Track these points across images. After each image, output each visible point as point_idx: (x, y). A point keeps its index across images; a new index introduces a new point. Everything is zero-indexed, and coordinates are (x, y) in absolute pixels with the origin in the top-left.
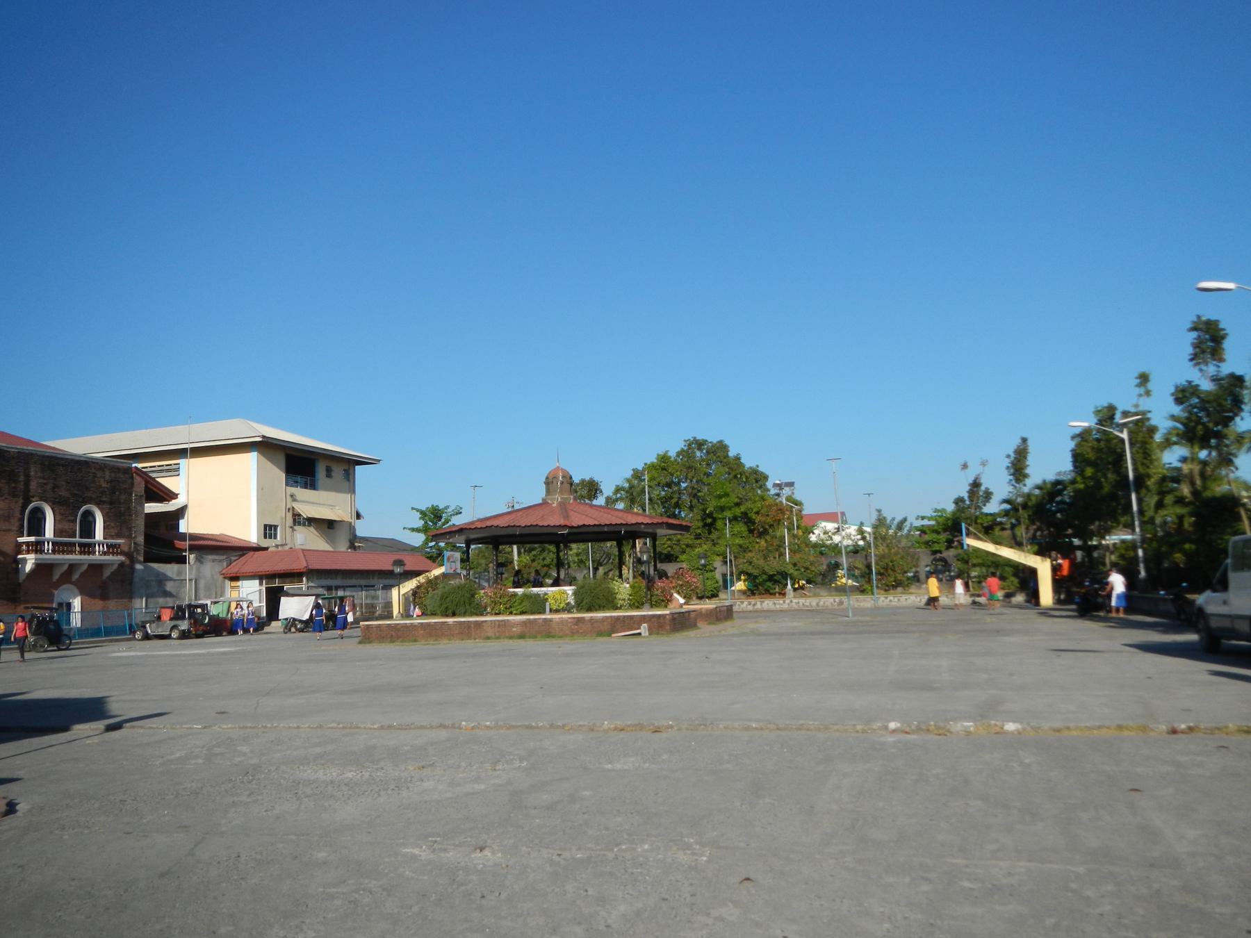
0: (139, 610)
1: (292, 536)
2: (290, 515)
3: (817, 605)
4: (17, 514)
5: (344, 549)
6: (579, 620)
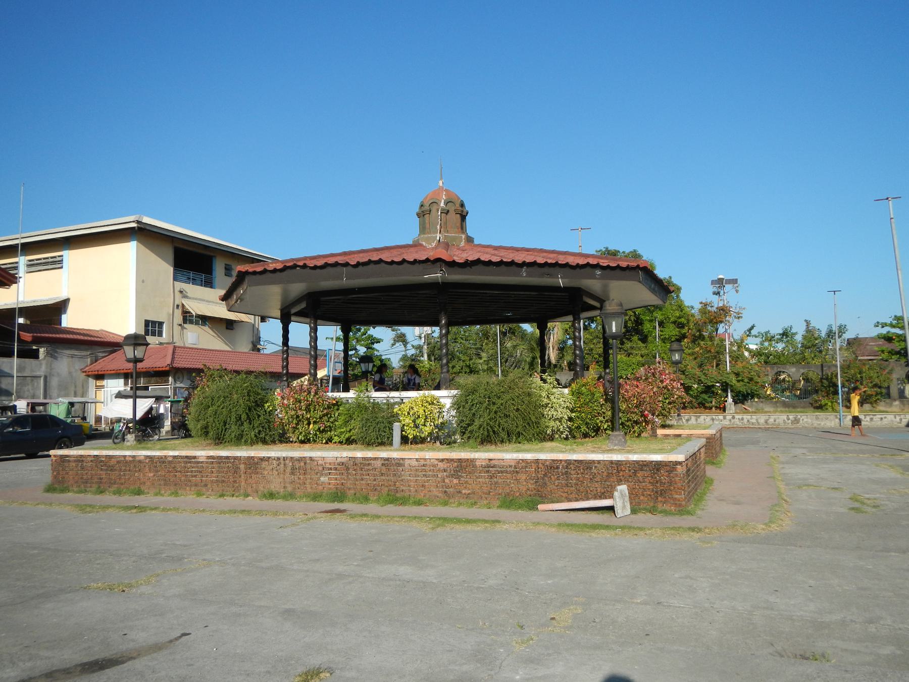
1: (182, 335)
2: (178, 314)
3: (766, 422)
5: (246, 350)
6: (463, 466)
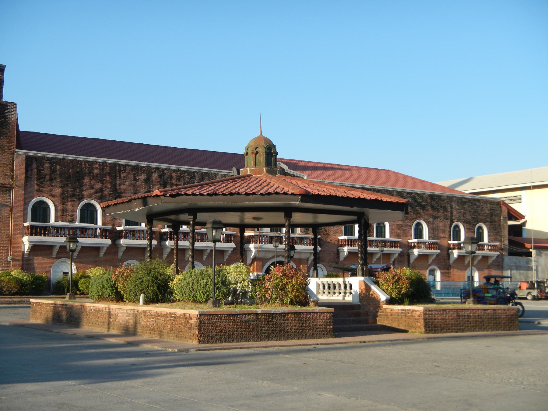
0: (507, 283)
4: (448, 229)
